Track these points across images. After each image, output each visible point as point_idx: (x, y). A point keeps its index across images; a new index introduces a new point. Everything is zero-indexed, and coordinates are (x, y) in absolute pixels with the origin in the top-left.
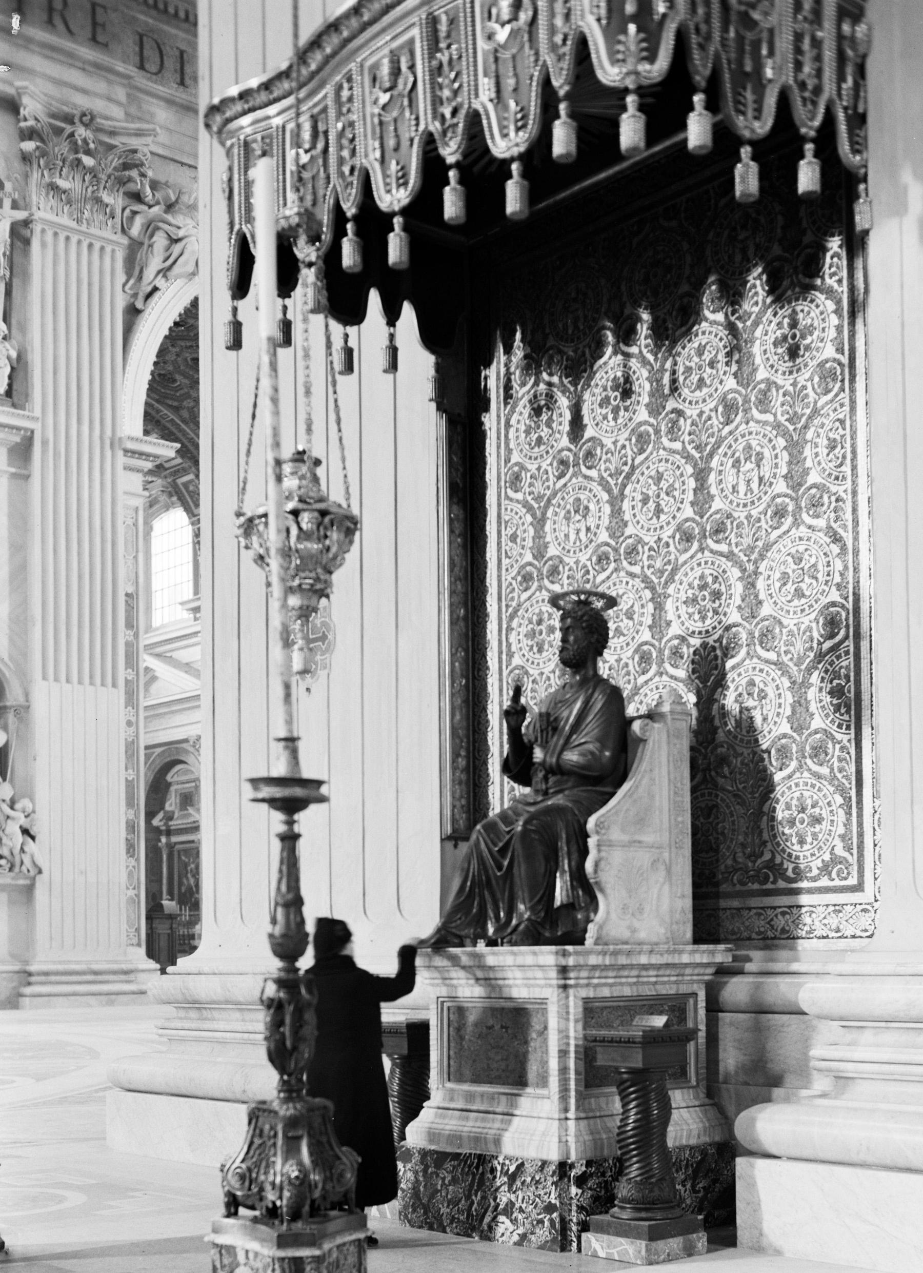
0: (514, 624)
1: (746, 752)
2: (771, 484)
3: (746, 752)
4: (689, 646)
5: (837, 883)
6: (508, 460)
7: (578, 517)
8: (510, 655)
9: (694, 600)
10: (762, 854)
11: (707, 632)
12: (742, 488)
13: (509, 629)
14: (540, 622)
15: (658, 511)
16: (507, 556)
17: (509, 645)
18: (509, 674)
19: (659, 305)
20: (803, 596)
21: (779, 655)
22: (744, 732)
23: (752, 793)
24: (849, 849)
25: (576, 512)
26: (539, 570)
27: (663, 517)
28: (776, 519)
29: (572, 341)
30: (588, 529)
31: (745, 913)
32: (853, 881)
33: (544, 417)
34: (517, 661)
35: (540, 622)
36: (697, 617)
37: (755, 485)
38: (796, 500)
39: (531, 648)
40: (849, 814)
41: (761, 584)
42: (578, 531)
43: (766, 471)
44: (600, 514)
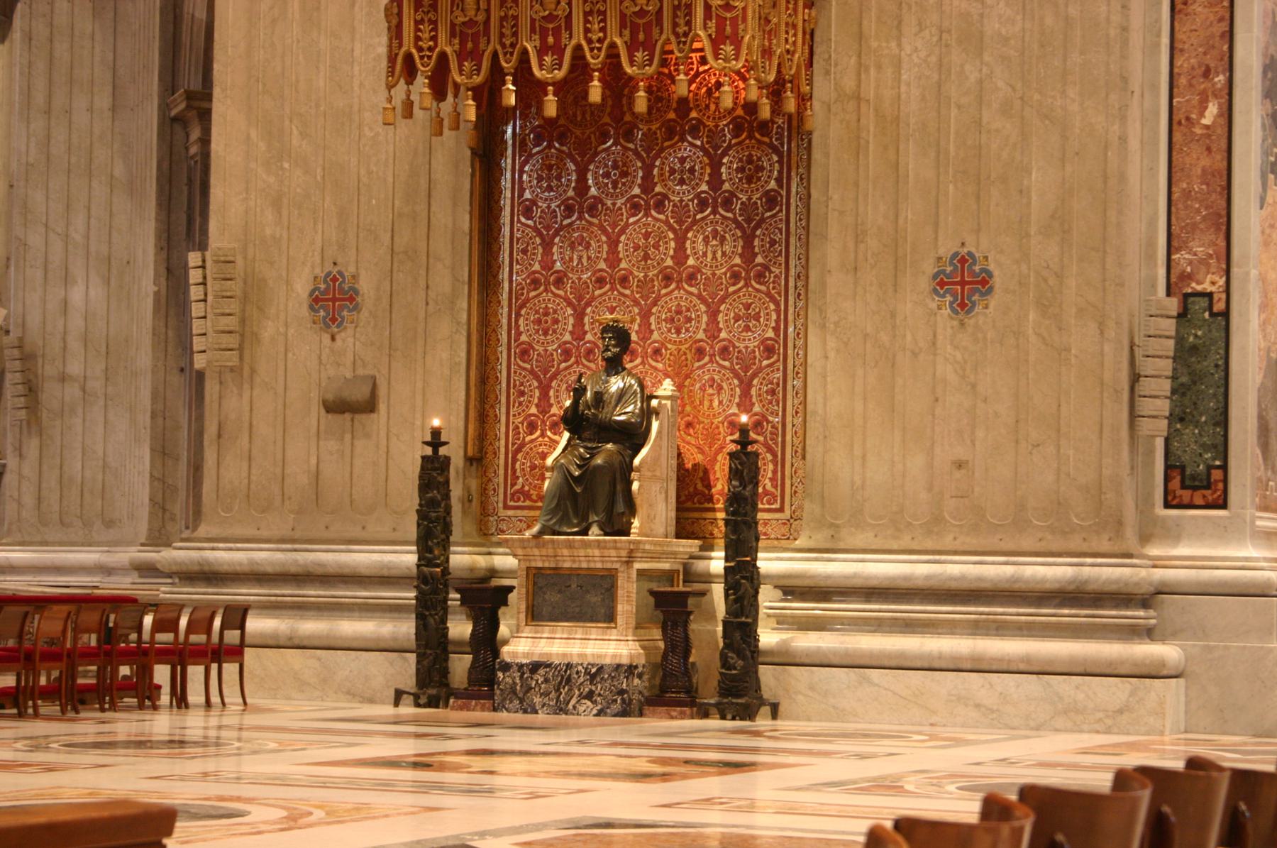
0: (523, 312)
1: (706, 421)
2: (730, 257)
3: (706, 421)
4: (667, 349)
5: (767, 506)
6: (521, 195)
7: (580, 248)
8: (519, 334)
9: (672, 320)
10: (715, 486)
11: (680, 342)
12: (710, 256)
13: (518, 315)
14: (546, 314)
15: (646, 257)
16: (518, 263)
17: (517, 326)
18: (518, 346)
19: (652, 121)
20: (750, 330)
21: (732, 363)
22: (706, 408)
23: (710, 447)
24: (776, 487)
25: (579, 244)
26: (546, 278)
27: (649, 262)
28: (733, 280)
29: (581, 126)
30: (589, 258)
31: (702, 521)
32: (777, 506)
33: (554, 173)
34: (524, 338)
35: (546, 314)
36: (673, 331)
37: (719, 254)
38: (748, 272)
39: (537, 331)
40: (776, 465)
41: (720, 318)
42: (580, 258)
43: (727, 248)
44: (599, 247)
